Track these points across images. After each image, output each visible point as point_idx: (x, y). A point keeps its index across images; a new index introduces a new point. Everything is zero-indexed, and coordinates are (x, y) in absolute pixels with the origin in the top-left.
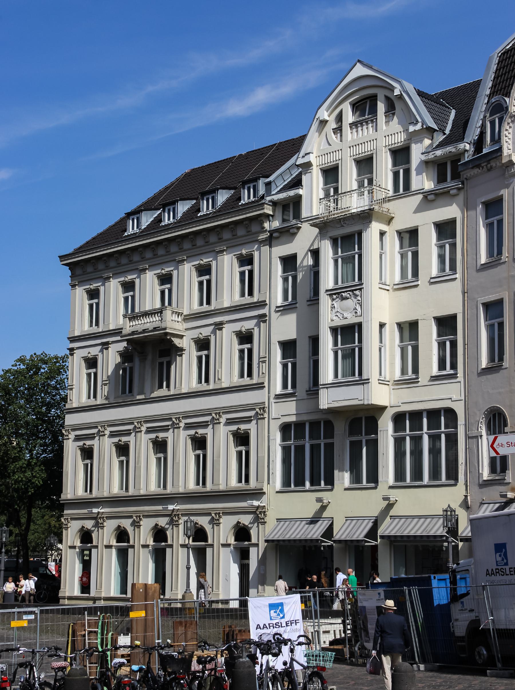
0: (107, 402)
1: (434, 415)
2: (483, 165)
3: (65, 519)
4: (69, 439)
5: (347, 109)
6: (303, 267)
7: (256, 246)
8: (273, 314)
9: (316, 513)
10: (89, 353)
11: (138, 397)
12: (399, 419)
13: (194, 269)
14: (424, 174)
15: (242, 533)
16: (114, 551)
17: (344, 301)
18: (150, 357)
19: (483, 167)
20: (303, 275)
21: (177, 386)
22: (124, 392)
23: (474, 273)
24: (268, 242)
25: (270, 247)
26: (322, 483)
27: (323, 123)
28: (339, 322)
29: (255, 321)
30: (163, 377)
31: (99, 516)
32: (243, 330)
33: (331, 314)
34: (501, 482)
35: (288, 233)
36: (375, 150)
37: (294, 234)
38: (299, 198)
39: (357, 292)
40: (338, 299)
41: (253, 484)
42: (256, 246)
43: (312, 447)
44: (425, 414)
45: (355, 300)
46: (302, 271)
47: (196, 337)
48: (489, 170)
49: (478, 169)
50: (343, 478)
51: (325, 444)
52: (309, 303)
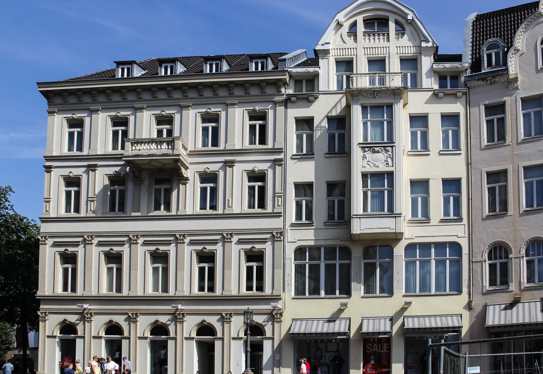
0: (94, 215)
1: (440, 246)
2: (488, 79)
3: (42, 313)
4: (46, 244)
5: (360, 20)
6: (321, 127)
7: (270, 106)
8: (289, 160)
9: (333, 314)
10: (71, 172)
11: (133, 214)
12: (411, 248)
13: (200, 116)
14: (433, 78)
15: (255, 330)
16: (103, 341)
17: (375, 154)
18: (146, 183)
19: (487, 81)
20: (321, 134)
21: (180, 208)
22: (112, 209)
23: (478, 151)
24: (284, 104)
25: (286, 107)
26: (337, 292)
27: (339, 25)
28: (370, 169)
29: (269, 164)
30: (162, 199)
31: (85, 312)
32: (256, 169)
33: (361, 162)
34: (505, 290)
35: (308, 99)
36: (388, 55)
37: (312, 102)
38: (316, 75)
39: (389, 148)
40: (369, 152)
41: (268, 290)
42: (270, 106)
43: (327, 266)
44: (433, 246)
45: (386, 155)
46: (321, 130)
47: (202, 170)
48: (491, 84)
49: (482, 82)
50: (358, 289)
51: (340, 265)
52: (326, 156)
